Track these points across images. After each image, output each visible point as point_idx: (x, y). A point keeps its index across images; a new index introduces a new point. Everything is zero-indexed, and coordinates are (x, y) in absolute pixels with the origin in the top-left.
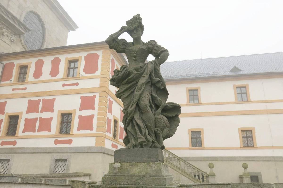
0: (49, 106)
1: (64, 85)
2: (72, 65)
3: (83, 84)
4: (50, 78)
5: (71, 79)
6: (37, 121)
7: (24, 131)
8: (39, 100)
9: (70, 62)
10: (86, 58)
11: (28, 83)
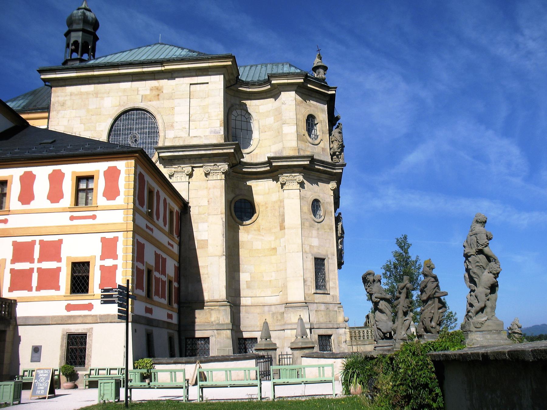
0: (52, 251)
1: (72, 218)
2: (83, 186)
3: (103, 217)
4: (48, 205)
5: (81, 209)
6: (33, 274)
7: (11, 290)
8: (34, 242)
9: (79, 179)
10: (105, 173)
11: (9, 212)
